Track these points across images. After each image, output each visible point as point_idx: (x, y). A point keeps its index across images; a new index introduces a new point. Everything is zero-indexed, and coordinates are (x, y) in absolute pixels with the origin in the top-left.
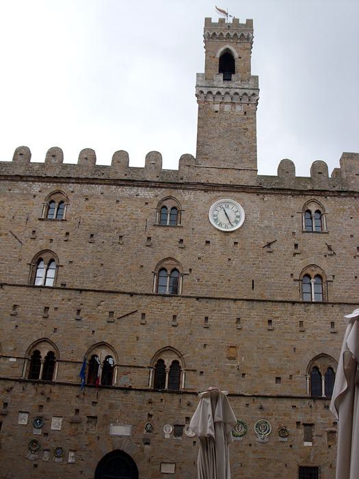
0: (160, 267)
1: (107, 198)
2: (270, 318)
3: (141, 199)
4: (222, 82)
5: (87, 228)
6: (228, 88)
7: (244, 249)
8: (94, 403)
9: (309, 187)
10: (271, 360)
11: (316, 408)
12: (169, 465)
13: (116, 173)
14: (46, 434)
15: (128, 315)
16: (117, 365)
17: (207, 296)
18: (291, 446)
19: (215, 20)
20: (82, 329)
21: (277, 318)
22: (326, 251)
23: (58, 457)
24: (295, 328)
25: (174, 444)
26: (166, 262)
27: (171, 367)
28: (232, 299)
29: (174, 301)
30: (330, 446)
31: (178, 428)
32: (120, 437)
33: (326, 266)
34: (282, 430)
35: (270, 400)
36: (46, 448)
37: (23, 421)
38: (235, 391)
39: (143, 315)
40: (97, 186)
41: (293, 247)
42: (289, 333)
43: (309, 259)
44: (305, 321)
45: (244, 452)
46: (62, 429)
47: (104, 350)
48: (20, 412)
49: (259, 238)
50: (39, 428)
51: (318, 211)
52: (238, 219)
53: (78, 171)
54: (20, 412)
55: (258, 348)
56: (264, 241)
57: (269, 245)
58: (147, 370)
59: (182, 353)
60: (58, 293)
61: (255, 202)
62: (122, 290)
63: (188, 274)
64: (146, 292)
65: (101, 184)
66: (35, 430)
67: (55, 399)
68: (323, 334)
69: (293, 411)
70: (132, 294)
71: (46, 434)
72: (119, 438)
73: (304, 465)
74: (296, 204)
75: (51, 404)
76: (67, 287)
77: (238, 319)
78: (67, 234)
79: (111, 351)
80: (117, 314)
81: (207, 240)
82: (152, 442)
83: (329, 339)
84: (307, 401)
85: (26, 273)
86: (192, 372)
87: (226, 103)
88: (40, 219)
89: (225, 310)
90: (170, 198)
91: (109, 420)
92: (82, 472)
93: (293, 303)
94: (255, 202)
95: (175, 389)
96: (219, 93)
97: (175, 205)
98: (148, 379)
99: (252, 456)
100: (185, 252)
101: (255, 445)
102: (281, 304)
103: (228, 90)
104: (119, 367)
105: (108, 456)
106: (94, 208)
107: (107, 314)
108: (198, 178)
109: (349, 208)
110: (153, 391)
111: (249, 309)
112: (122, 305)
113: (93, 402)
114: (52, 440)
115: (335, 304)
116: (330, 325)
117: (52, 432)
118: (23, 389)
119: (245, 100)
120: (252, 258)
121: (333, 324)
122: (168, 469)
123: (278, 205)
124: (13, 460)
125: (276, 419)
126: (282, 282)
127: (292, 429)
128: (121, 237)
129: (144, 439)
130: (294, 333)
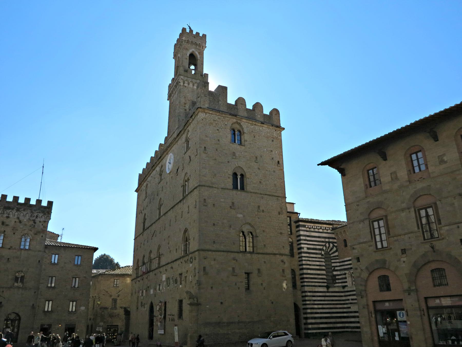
35: (175, 263)
93: (180, 201)
110: (156, 269)
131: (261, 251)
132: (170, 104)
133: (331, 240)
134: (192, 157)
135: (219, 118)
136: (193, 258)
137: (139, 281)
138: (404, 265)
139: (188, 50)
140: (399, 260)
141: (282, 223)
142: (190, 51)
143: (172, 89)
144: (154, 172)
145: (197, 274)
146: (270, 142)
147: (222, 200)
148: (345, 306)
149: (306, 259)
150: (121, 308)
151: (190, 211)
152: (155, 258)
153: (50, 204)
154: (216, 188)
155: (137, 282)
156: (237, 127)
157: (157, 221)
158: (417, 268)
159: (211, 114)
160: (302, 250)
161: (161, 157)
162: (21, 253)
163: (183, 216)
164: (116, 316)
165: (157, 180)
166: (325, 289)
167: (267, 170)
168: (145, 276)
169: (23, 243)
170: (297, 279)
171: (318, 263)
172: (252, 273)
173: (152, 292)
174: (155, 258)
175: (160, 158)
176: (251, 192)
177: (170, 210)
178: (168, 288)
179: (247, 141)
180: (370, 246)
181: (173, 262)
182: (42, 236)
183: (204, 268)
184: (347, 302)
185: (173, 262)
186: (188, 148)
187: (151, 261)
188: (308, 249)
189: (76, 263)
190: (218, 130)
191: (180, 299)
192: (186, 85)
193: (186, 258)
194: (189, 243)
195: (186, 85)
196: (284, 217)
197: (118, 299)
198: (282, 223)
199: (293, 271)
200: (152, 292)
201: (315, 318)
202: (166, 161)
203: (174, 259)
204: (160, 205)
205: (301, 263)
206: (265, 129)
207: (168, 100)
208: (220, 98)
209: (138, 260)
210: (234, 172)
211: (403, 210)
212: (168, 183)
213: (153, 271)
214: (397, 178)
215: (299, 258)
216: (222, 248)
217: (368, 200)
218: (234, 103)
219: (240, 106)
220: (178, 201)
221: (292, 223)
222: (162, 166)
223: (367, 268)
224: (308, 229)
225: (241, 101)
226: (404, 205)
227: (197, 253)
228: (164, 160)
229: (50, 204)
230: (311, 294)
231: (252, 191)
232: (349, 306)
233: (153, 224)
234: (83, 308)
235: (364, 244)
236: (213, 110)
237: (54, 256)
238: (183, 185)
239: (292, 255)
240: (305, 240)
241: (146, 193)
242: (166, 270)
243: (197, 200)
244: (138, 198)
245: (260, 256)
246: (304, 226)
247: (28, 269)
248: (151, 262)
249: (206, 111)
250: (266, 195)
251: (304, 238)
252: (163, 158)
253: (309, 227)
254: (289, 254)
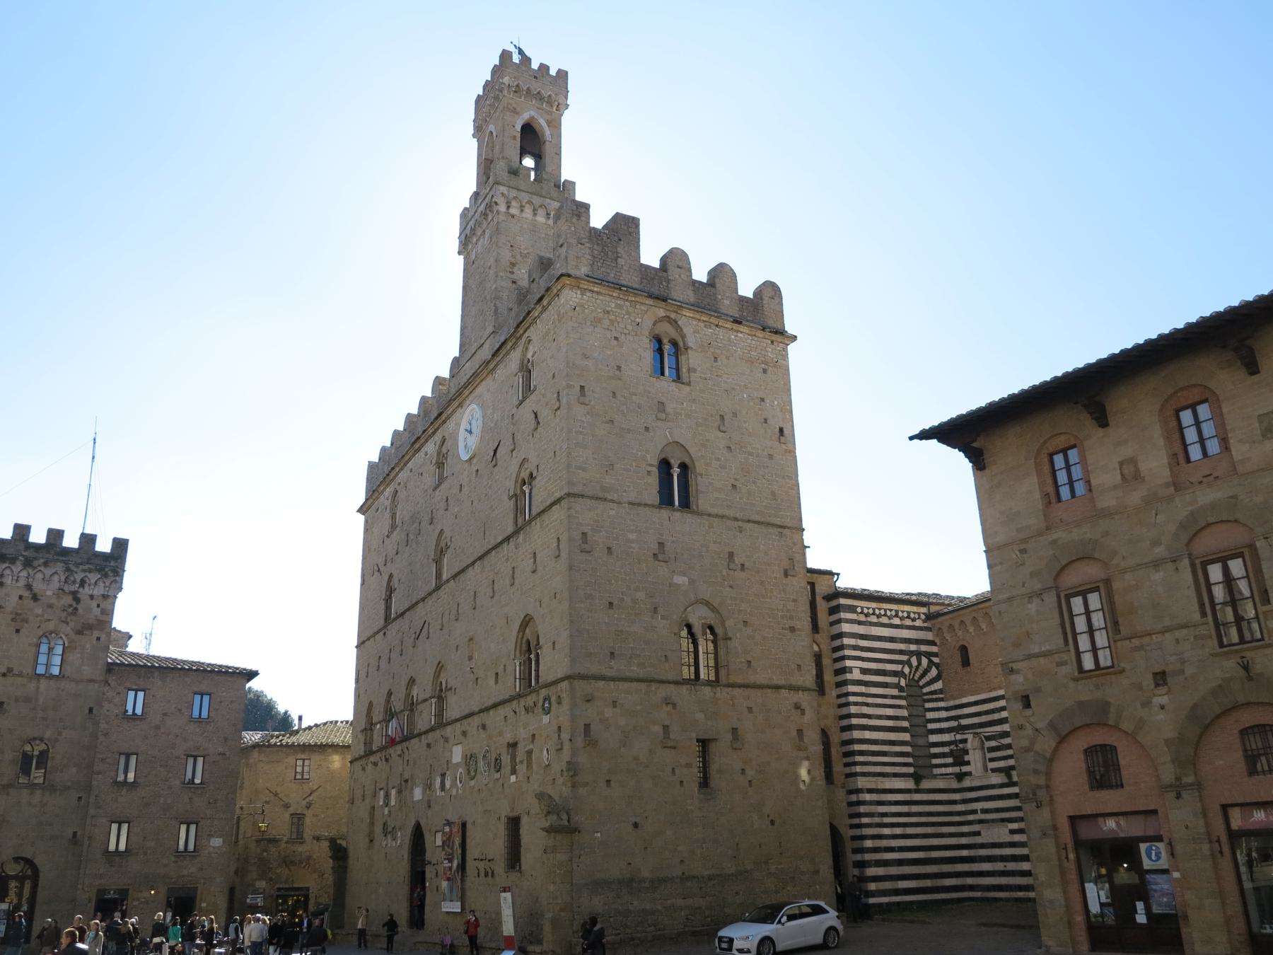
35: (491, 712)
57: (495, 451)
73: (511, 815)
93: (507, 539)
110: (432, 729)
131: (739, 680)
132: (465, 265)
133: (923, 648)
134: (545, 414)
135: (618, 306)
136: (553, 699)
137: (375, 764)
138: (1162, 718)
139: (518, 113)
140: (1147, 704)
141: (794, 601)
142: (520, 117)
143: (472, 223)
144: (419, 457)
145: (567, 745)
146: (760, 374)
147: (632, 536)
148: (965, 829)
149: (859, 699)
150: (318, 839)
151: (540, 568)
152: (426, 700)
153: (120, 546)
154: (613, 501)
155: (370, 767)
156: (667, 330)
157: (430, 594)
158: (1200, 727)
159: (598, 293)
160: (849, 676)
161: (440, 414)
162: (38, 688)
163: (517, 582)
164: (301, 862)
165: (429, 480)
166: (910, 784)
167: (750, 454)
168: (395, 751)
169: (42, 659)
170: (837, 755)
171: (890, 712)
172: (715, 740)
173: (418, 794)
174: (426, 700)
175: (436, 418)
176: (709, 515)
177: (473, 563)
178: (472, 783)
179: (695, 371)
180: (1059, 664)
181: (487, 709)
182: (98, 639)
183: (587, 726)
184: (971, 817)
185: (487, 709)
186: (528, 389)
187: (412, 706)
188: (864, 671)
189: (196, 714)
190: (616, 338)
191: (514, 814)
192: (513, 211)
193: (530, 700)
194: (537, 655)
195: (513, 211)
196: (798, 584)
197: (309, 813)
198: (794, 601)
199: (824, 733)
200: (418, 794)
201: (886, 863)
202: (458, 425)
203: (490, 703)
204: (441, 552)
205: (844, 711)
206: (743, 338)
207: (460, 253)
208: (619, 250)
209: (371, 704)
210: (663, 456)
211: (1157, 564)
212: (466, 489)
213: (419, 735)
214: (1138, 477)
215: (839, 696)
216: (635, 670)
217: (1055, 536)
218: (657, 265)
219: (673, 273)
220: (500, 539)
221: (819, 599)
222: (444, 441)
223: (1052, 726)
224: (862, 618)
225: (675, 260)
226: (1160, 551)
227: (565, 684)
228: (451, 425)
229: (120, 546)
230: (874, 797)
231: (712, 511)
232: (976, 828)
233: (417, 603)
234: (217, 842)
235: (1041, 659)
236: (601, 281)
237: (131, 694)
238: (515, 495)
239: (821, 689)
240: (855, 648)
241: (393, 517)
242: (464, 733)
243: (564, 538)
244: (366, 530)
245: (737, 692)
246: (852, 609)
247: (60, 734)
248: (412, 710)
249: (584, 285)
250: (749, 521)
251: (851, 641)
252: (448, 418)
253: (866, 611)
254: (814, 686)
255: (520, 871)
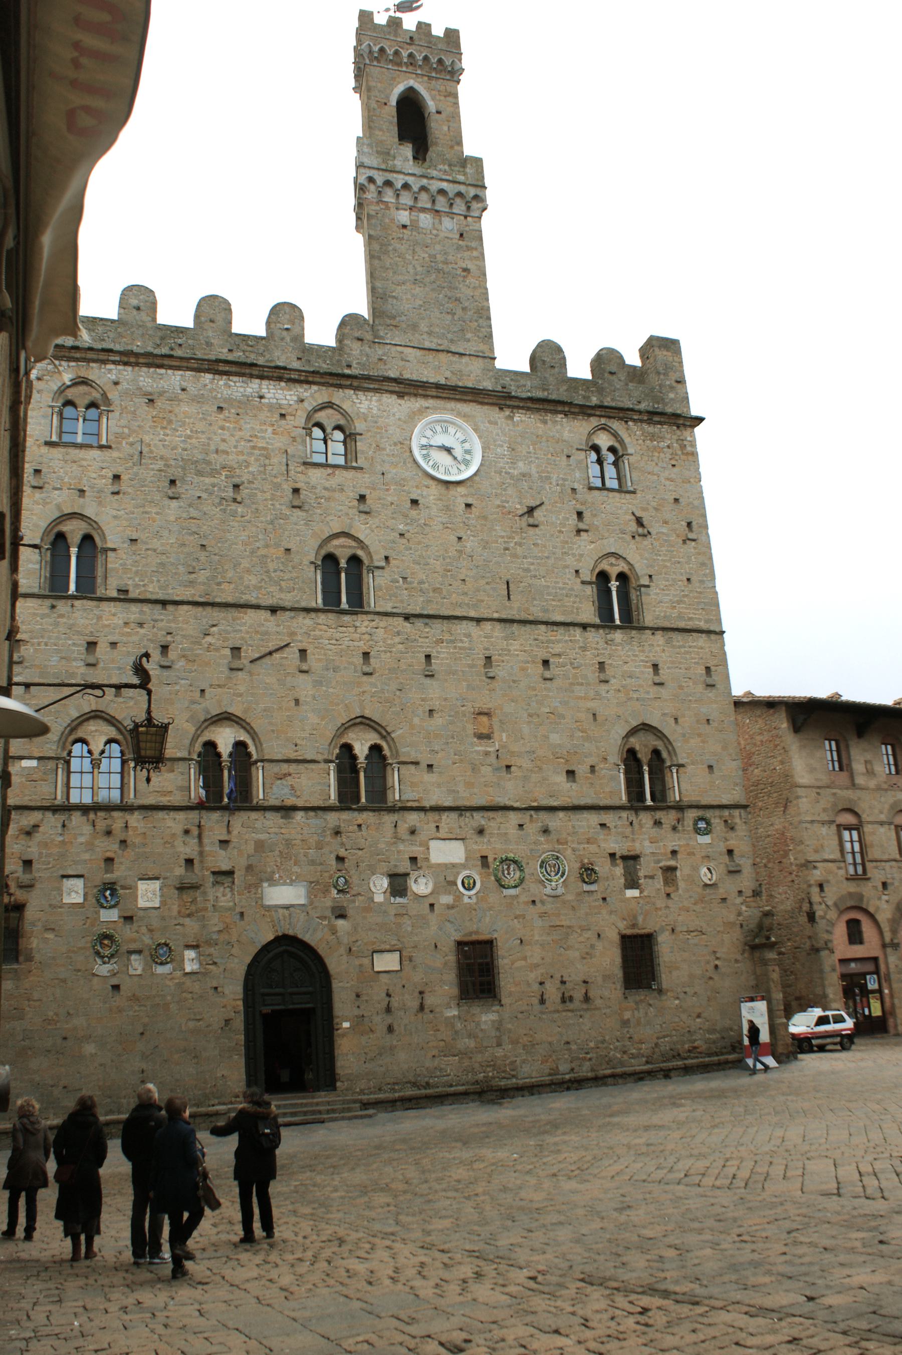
0: (323, 552)
1: (198, 400)
2: (546, 656)
3: (271, 407)
4: (411, 162)
5: (160, 464)
6: (426, 177)
7: (485, 518)
8: (224, 843)
9: (594, 400)
10: (555, 738)
11: (641, 826)
12: (387, 956)
13: (209, 344)
14: (128, 919)
15: (270, 653)
16: (262, 761)
17: (425, 612)
18: (604, 899)
19: (381, 19)
20: (177, 687)
21: (559, 655)
22: (633, 526)
23: (162, 964)
24: (592, 675)
25: (393, 912)
26: (336, 542)
27: (367, 758)
28: (471, 619)
29: (363, 623)
30: (668, 895)
31: (400, 880)
32: (287, 907)
33: (638, 558)
34: (587, 869)
35: (561, 814)
36: (133, 946)
37: (73, 895)
38: (499, 799)
39: (303, 652)
40: (170, 372)
41: (575, 516)
42: (582, 684)
43: (605, 542)
44: (608, 662)
45: (523, 917)
46: (161, 902)
47: (228, 730)
48: (64, 876)
49: (511, 496)
50: (111, 907)
51: (612, 449)
52: (468, 457)
53: (121, 335)
54: (64, 876)
55: (530, 715)
56: (520, 503)
57: (531, 511)
58: (325, 766)
59: (389, 729)
60: (113, 610)
61: (496, 423)
62: (254, 601)
63: (383, 568)
64: (303, 604)
65: (178, 368)
66: (102, 911)
67: (137, 840)
68: (641, 686)
69: (602, 835)
70: (274, 610)
71: (128, 919)
72: (286, 912)
73: (629, 932)
74: (574, 430)
75: (130, 853)
76: (132, 595)
77: (488, 658)
78: (117, 477)
79: (242, 731)
80: (249, 653)
81: (414, 497)
82: (350, 912)
83: (652, 696)
84: (624, 814)
85: (31, 566)
86: (412, 767)
87: (423, 210)
88: (49, 444)
89: (461, 641)
90: (329, 405)
91: (258, 876)
92: (216, 988)
93: (584, 627)
94: (496, 423)
95: (379, 801)
96: (406, 186)
97: (342, 422)
98: (328, 785)
99: (538, 923)
100: (373, 521)
101: (543, 902)
102: (561, 630)
103: (425, 182)
104: (266, 764)
105: (266, 948)
106: (170, 422)
107: (228, 652)
108: (381, 366)
109: (668, 447)
111: (506, 638)
112: (257, 632)
113: (221, 841)
114: (144, 930)
115: (657, 629)
116: (651, 670)
117: (141, 913)
118: (64, 826)
119: (459, 207)
120: (503, 537)
121: (655, 667)
122: (387, 962)
123: (540, 432)
124: (64, 981)
125: (574, 850)
126: (561, 585)
127: (603, 867)
128: (236, 487)
129: (333, 909)
130: (588, 684)
177: (478, 620)
180: (839, 868)
211: (882, 824)
213: (286, 810)
223: (836, 904)
227: (736, 812)
255: (660, 991)
